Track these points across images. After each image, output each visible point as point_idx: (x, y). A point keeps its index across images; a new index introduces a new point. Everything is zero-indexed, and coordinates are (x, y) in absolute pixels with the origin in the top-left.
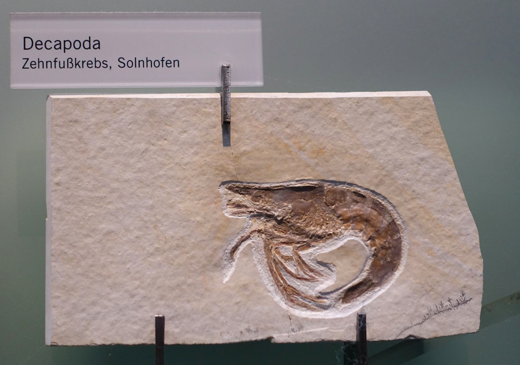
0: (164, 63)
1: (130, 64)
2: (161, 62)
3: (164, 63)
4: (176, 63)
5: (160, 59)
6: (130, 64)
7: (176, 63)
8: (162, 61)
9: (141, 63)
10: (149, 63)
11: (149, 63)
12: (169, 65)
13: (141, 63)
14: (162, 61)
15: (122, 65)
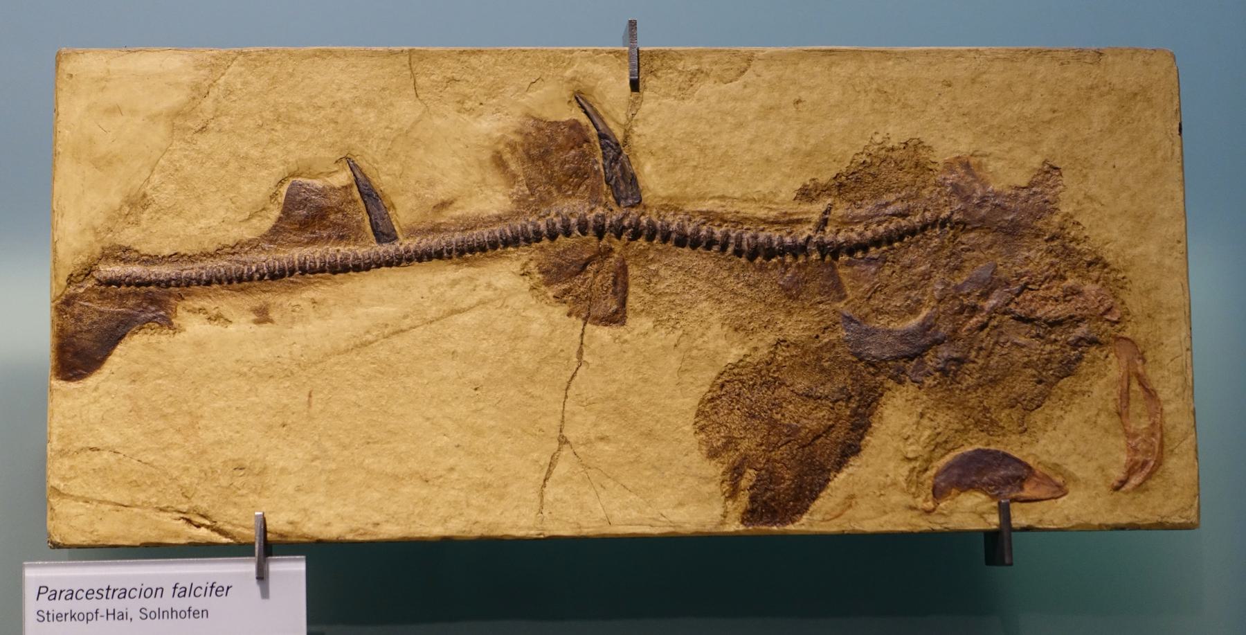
0: (191, 613)
1: (153, 615)
2: (187, 613)
3: (191, 613)
4: (205, 613)
5: (186, 609)
6: (153, 615)
7: (205, 613)
8: (189, 610)
9: (166, 614)
10: (174, 614)
11: (174, 614)
12: (196, 616)
13: (166, 614)
14: (189, 610)
15: (144, 616)
